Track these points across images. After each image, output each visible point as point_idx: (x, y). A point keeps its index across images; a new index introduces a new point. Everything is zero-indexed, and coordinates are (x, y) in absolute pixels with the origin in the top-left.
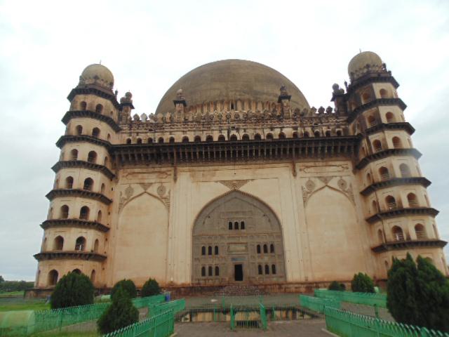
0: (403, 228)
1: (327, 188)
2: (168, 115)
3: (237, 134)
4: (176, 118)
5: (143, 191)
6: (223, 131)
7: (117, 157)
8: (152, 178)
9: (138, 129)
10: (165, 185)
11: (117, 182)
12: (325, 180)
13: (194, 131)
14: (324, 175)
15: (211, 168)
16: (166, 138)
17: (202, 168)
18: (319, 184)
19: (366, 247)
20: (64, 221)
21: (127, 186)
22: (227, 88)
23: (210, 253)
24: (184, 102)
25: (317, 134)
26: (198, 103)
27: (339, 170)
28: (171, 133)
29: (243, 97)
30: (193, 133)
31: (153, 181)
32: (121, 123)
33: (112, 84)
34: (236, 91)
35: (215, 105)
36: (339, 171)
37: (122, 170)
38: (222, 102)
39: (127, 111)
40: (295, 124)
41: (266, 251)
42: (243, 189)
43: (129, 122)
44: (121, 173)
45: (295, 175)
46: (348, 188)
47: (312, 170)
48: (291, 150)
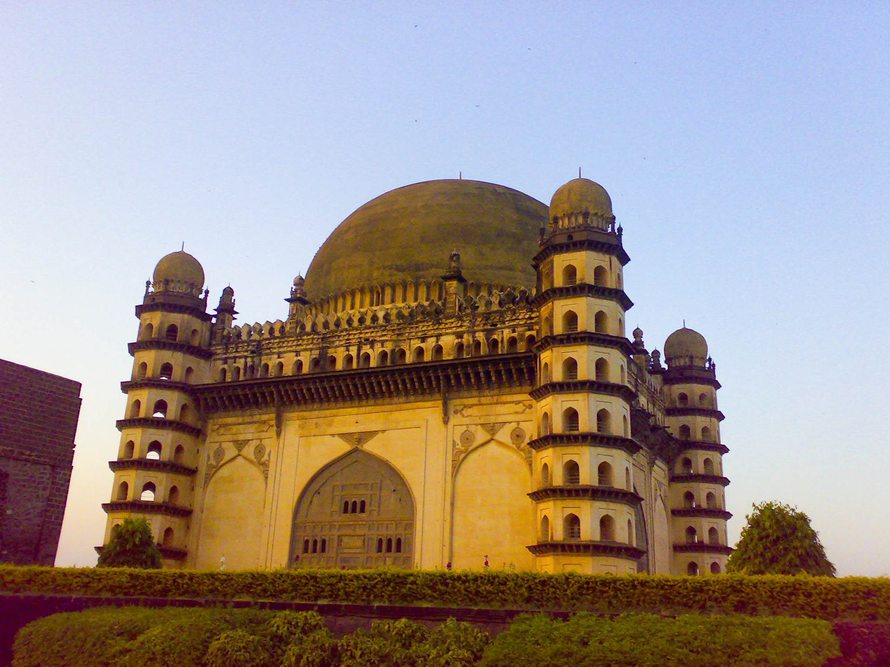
0: (550, 519)
1: (493, 444)
3: (370, 351)
5: (237, 453)
6: (351, 348)
7: (202, 402)
8: (248, 432)
9: (237, 352)
10: (265, 442)
11: (204, 441)
12: (492, 429)
14: (492, 419)
15: (328, 412)
16: (273, 362)
17: (316, 413)
18: (481, 436)
20: (120, 504)
21: (217, 445)
22: (371, 264)
23: (314, 551)
25: (495, 342)
26: (345, 288)
27: (518, 412)
29: (394, 279)
30: (309, 353)
31: (250, 437)
32: (214, 343)
34: (384, 268)
36: (517, 413)
37: (211, 421)
38: (362, 291)
40: (461, 326)
41: (389, 549)
42: (370, 446)
44: (211, 425)
45: (446, 422)
47: (474, 411)
48: (437, 378)
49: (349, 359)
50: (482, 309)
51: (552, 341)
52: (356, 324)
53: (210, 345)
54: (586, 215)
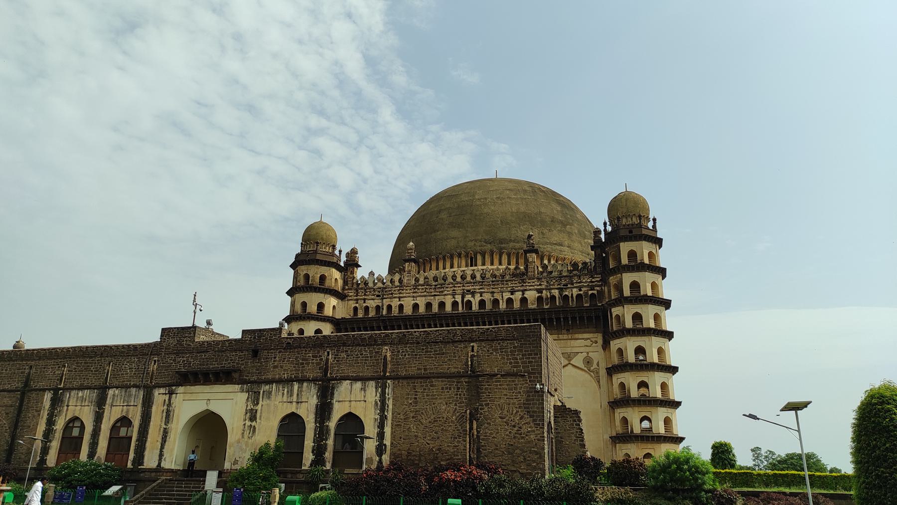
2: (397, 277)
3: (472, 299)
4: (405, 281)
12: (569, 357)
13: (425, 296)
14: (569, 350)
16: (395, 303)
19: (607, 437)
24: (414, 261)
28: (400, 298)
33: (334, 247)
34: (476, 241)
35: (452, 258)
38: (459, 256)
39: (352, 273)
40: (540, 285)
43: (355, 286)
46: (595, 366)
49: (455, 304)
50: (555, 274)
51: (622, 301)
52: (459, 279)
53: (343, 289)
54: (640, 216)
